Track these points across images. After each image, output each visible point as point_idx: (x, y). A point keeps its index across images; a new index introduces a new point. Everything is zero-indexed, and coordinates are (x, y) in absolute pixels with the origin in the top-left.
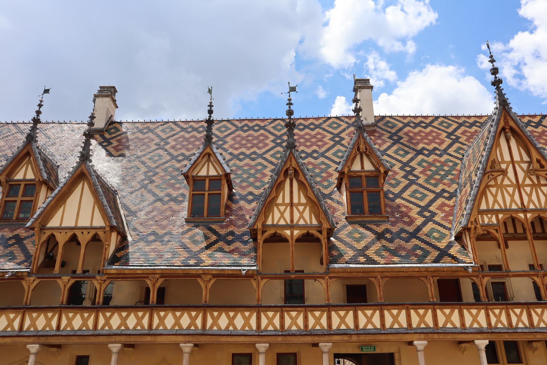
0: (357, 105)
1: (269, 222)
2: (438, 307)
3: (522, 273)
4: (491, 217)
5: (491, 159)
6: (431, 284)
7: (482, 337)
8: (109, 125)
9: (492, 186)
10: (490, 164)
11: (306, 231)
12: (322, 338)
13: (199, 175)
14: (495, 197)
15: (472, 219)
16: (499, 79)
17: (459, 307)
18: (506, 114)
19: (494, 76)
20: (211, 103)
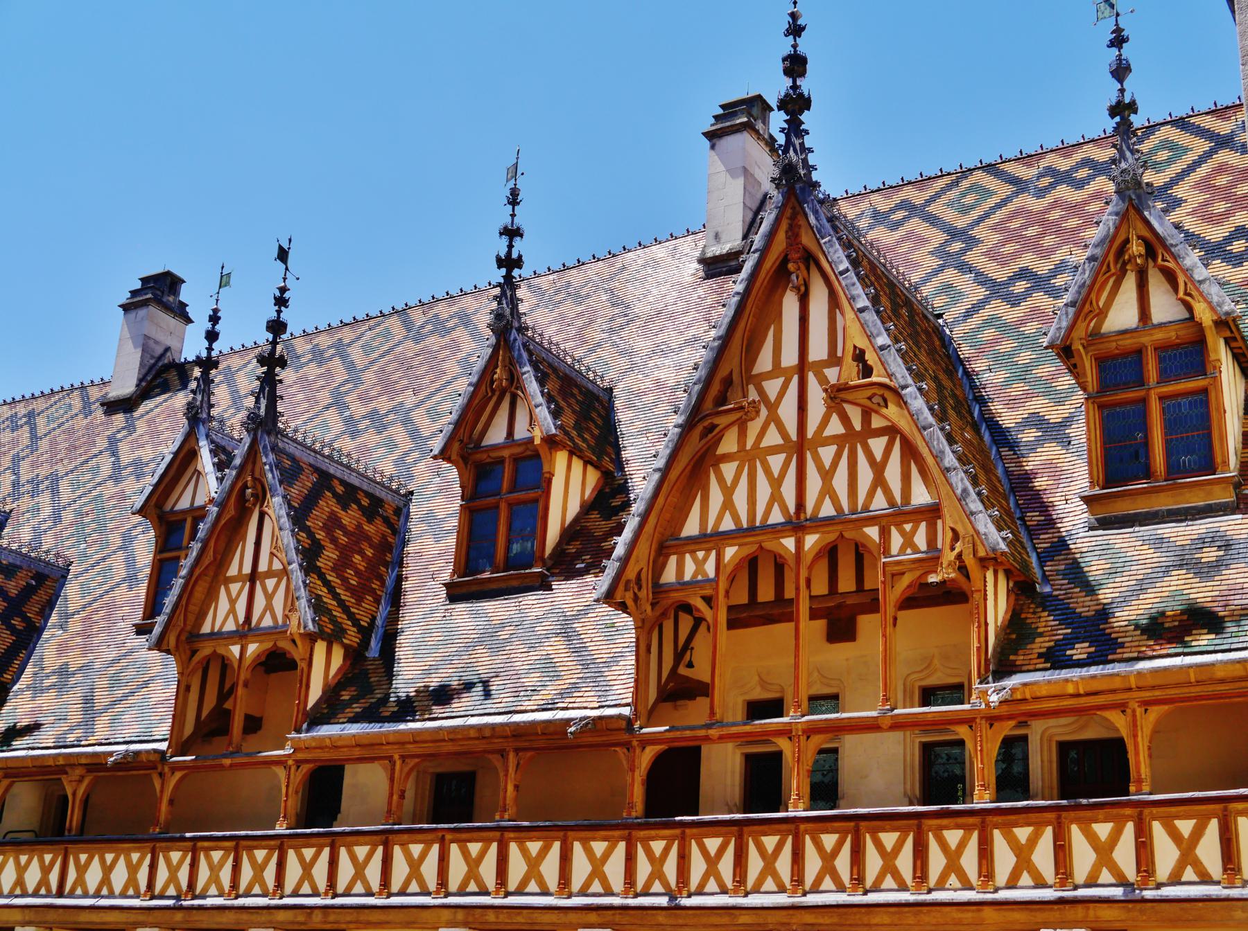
0: (510, 246)
1: (206, 629)
2: (512, 835)
3: (1052, 705)
4: (705, 559)
5: (723, 373)
6: (507, 771)
7: (600, 920)
8: (154, 378)
9: (727, 458)
10: (716, 388)
11: (268, 645)
12: (254, 917)
13: (177, 508)
14: (728, 492)
15: (631, 573)
16: (802, 95)
17: (561, 834)
18: (798, 208)
19: (789, 82)
20: (216, 311)
